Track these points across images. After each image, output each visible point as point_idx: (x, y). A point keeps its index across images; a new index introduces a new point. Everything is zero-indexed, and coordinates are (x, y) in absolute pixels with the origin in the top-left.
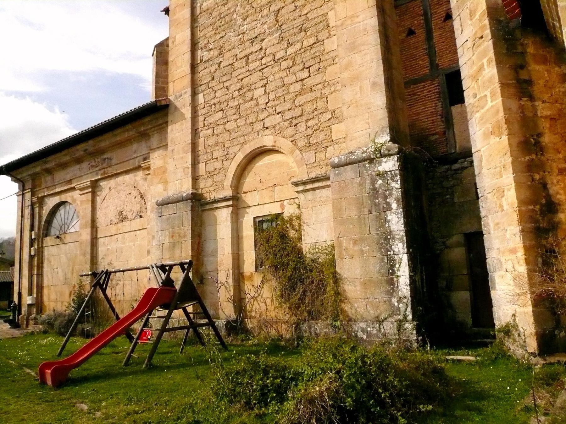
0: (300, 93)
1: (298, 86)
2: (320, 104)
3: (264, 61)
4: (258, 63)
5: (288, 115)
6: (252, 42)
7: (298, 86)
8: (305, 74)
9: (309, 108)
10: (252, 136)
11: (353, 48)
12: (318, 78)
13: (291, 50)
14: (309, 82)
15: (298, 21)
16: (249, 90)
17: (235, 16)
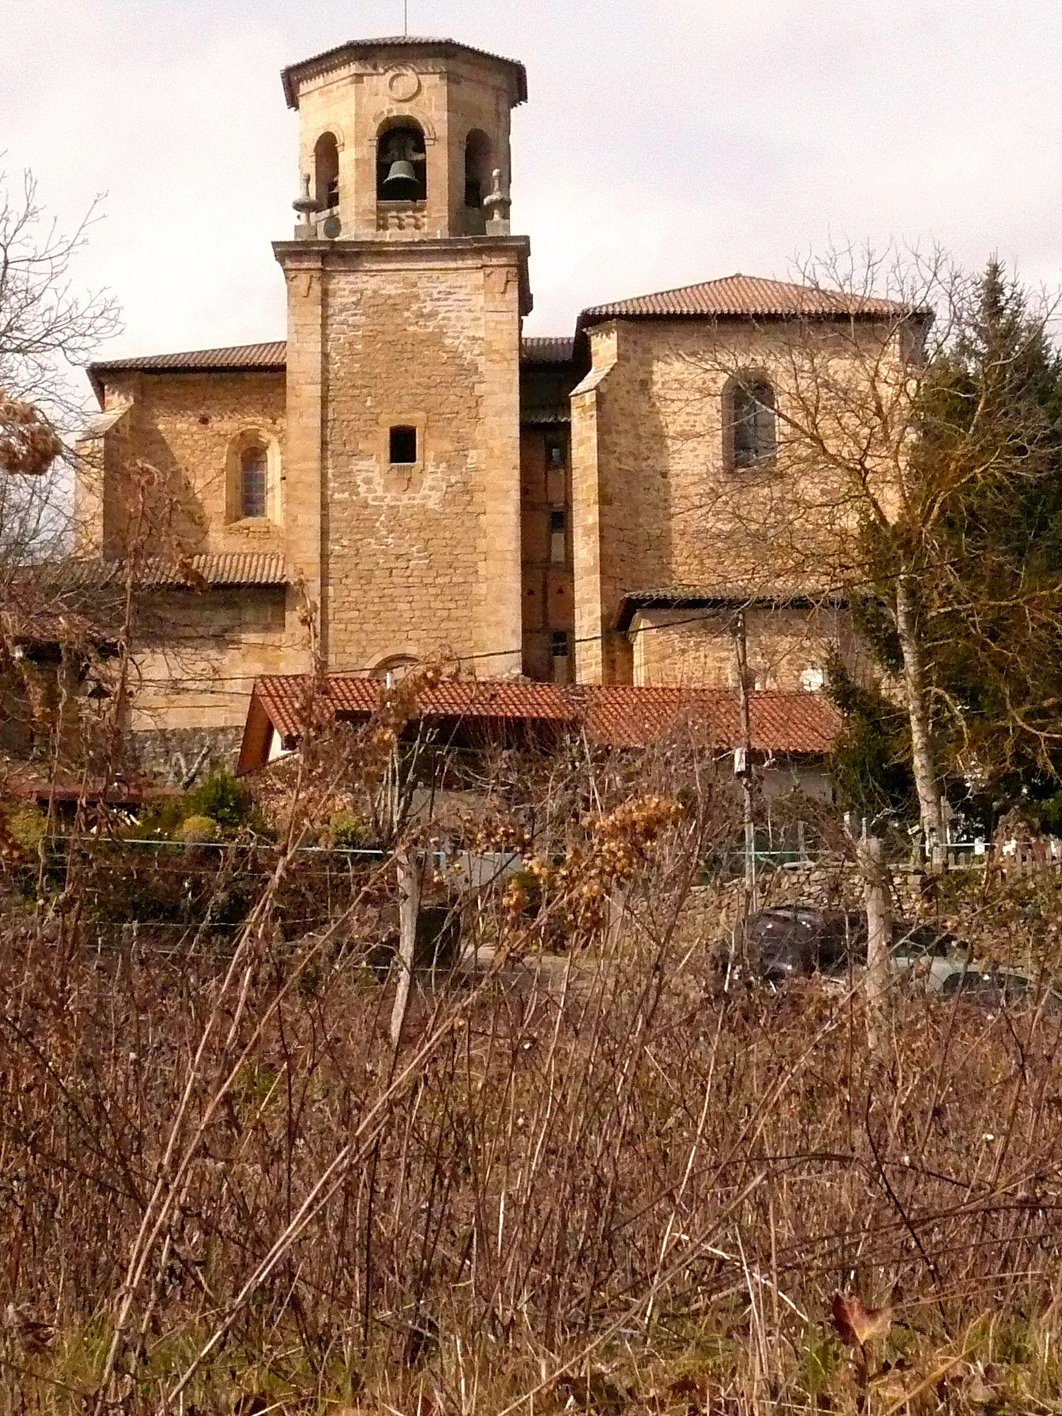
0: (449, 618)
1: (445, 613)
2: (466, 634)
3: (410, 580)
4: (404, 580)
5: (435, 634)
6: (397, 558)
7: (445, 613)
8: (452, 605)
9: (454, 634)
10: (394, 643)
11: (499, 600)
12: (465, 612)
13: (439, 580)
14: (455, 613)
15: (449, 558)
16: (392, 601)
17: (378, 524)
